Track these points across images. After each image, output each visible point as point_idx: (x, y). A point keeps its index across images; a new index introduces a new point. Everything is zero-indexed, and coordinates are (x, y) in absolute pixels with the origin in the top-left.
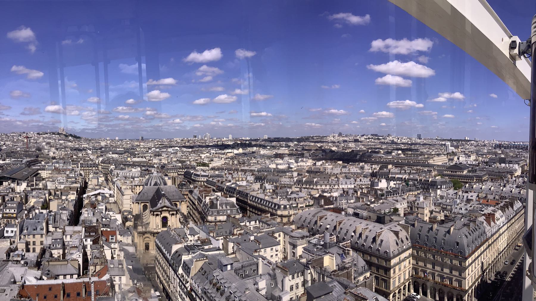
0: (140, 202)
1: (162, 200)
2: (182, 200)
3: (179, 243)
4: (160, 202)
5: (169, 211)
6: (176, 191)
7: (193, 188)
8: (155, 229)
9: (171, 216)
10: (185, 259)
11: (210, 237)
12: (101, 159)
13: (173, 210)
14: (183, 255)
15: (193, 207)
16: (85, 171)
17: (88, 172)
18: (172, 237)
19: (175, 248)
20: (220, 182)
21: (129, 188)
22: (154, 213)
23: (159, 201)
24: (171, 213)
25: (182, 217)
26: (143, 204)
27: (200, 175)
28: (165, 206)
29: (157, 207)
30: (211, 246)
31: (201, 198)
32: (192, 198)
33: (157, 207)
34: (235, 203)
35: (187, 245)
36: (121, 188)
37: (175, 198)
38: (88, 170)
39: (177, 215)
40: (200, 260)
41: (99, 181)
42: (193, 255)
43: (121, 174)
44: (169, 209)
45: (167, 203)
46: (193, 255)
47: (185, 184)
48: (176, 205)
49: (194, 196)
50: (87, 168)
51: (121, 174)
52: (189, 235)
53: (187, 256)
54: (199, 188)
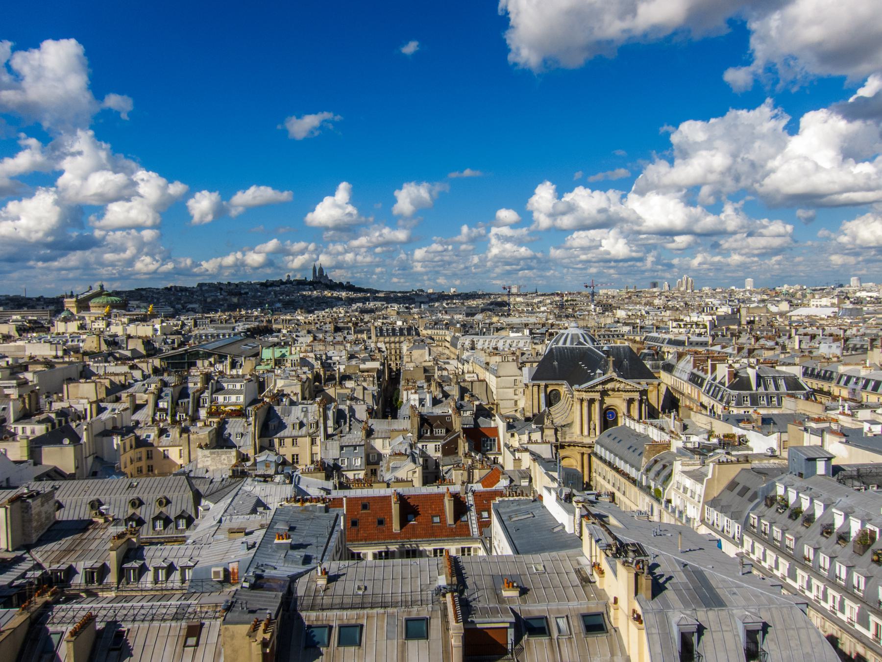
20: (745, 351)
28: (611, 380)
36: (488, 364)
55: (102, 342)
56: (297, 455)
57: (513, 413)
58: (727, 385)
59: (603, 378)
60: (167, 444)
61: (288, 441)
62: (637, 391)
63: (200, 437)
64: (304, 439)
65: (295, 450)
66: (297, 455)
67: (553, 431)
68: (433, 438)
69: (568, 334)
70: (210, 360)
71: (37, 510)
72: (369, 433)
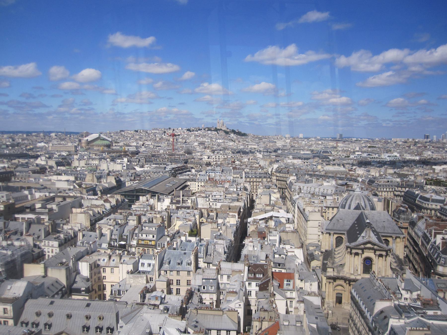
0: (332, 232)
1: (366, 232)
2: (398, 235)
3: (386, 300)
4: (363, 234)
5: (375, 250)
6: (388, 220)
7: (416, 218)
8: (351, 274)
9: (377, 257)
10: (395, 324)
11: (438, 299)
12: (275, 166)
13: (383, 249)
14: (391, 318)
15: (414, 248)
16: (252, 183)
17: (256, 186)
18: (377, 289)
19: (380, 305)
21: (317, 211)
22: (351, 251)
23: (360, 234)
24: (378, 253)
25: (396, 262)
26: (336, 236)
27: (429, 199)
28: (369, 242)
29: (357, 243)
30: (439, 313)
31: (429, 236)
32: (413, 234)
33: (357, 243)
35: (399, 305)
36: (304, 210)
37: (386, 231)
38: (256, 182)
39: (388, 257)
40: (416, 330)
41: (272, 198)
42: (408, 321)
43: (305, 188)
44: (375, 247)
45: (374, 239)
46: (408, 321)
47: (403, 211)
48: (387, 242)
49: (416, 230)
50: (255, 180)
51: (305, 188)
52: (403, 289)
53: (397, 320)
54: (426, 220)
55: (95, 177)
56: (179, 280)
57: (317, 242)
58: (441, 250)
59: (365, 240)
60: (113, 266)
65: (178, 278)
66: (179, 280)
67: (332, 269)
68: (255, 279)
70: (147, 196)
72: (218, 271)
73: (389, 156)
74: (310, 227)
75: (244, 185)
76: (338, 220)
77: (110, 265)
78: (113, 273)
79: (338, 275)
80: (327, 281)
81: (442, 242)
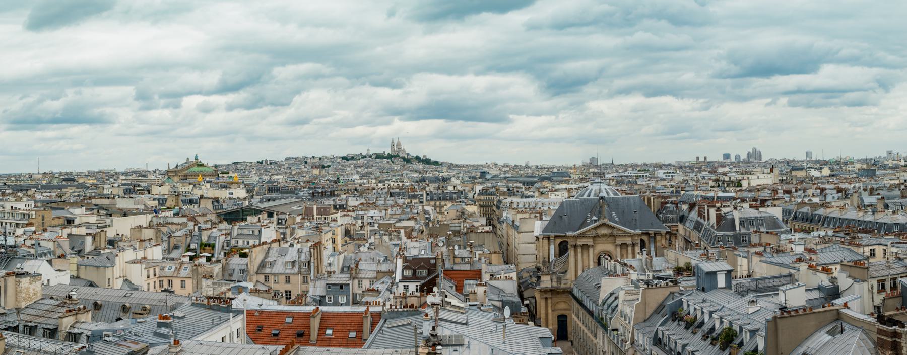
9: (619, 250)
12: (478, 188)
28: (604, 225)
31: (702, 221)
34: (780, 218)
36: (513, 221)
61: (282, 279)
62: (628, 236)
63: (207, 270)
64: (296, 276)
65: (288, 287)
66: (290, 292)
69: (592, 189)
71: (26, 285)
73: (664, 173)
74: (523, 243)
75: (423, 208)
76: (561, 217)
77: (179, 276)
78: (185, 287)
79: (559, 285)
80: (542, 296)
81: (717, 214)
